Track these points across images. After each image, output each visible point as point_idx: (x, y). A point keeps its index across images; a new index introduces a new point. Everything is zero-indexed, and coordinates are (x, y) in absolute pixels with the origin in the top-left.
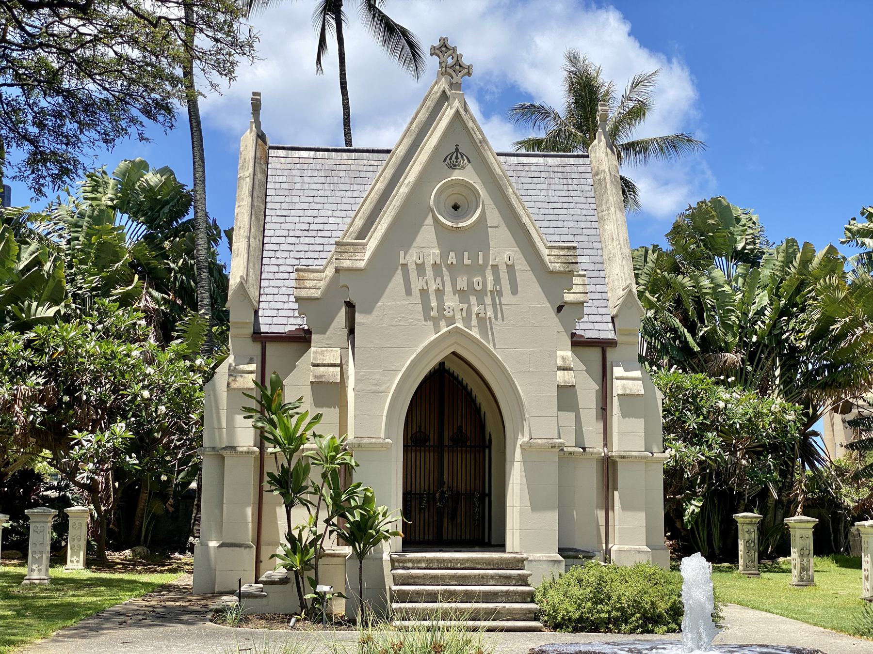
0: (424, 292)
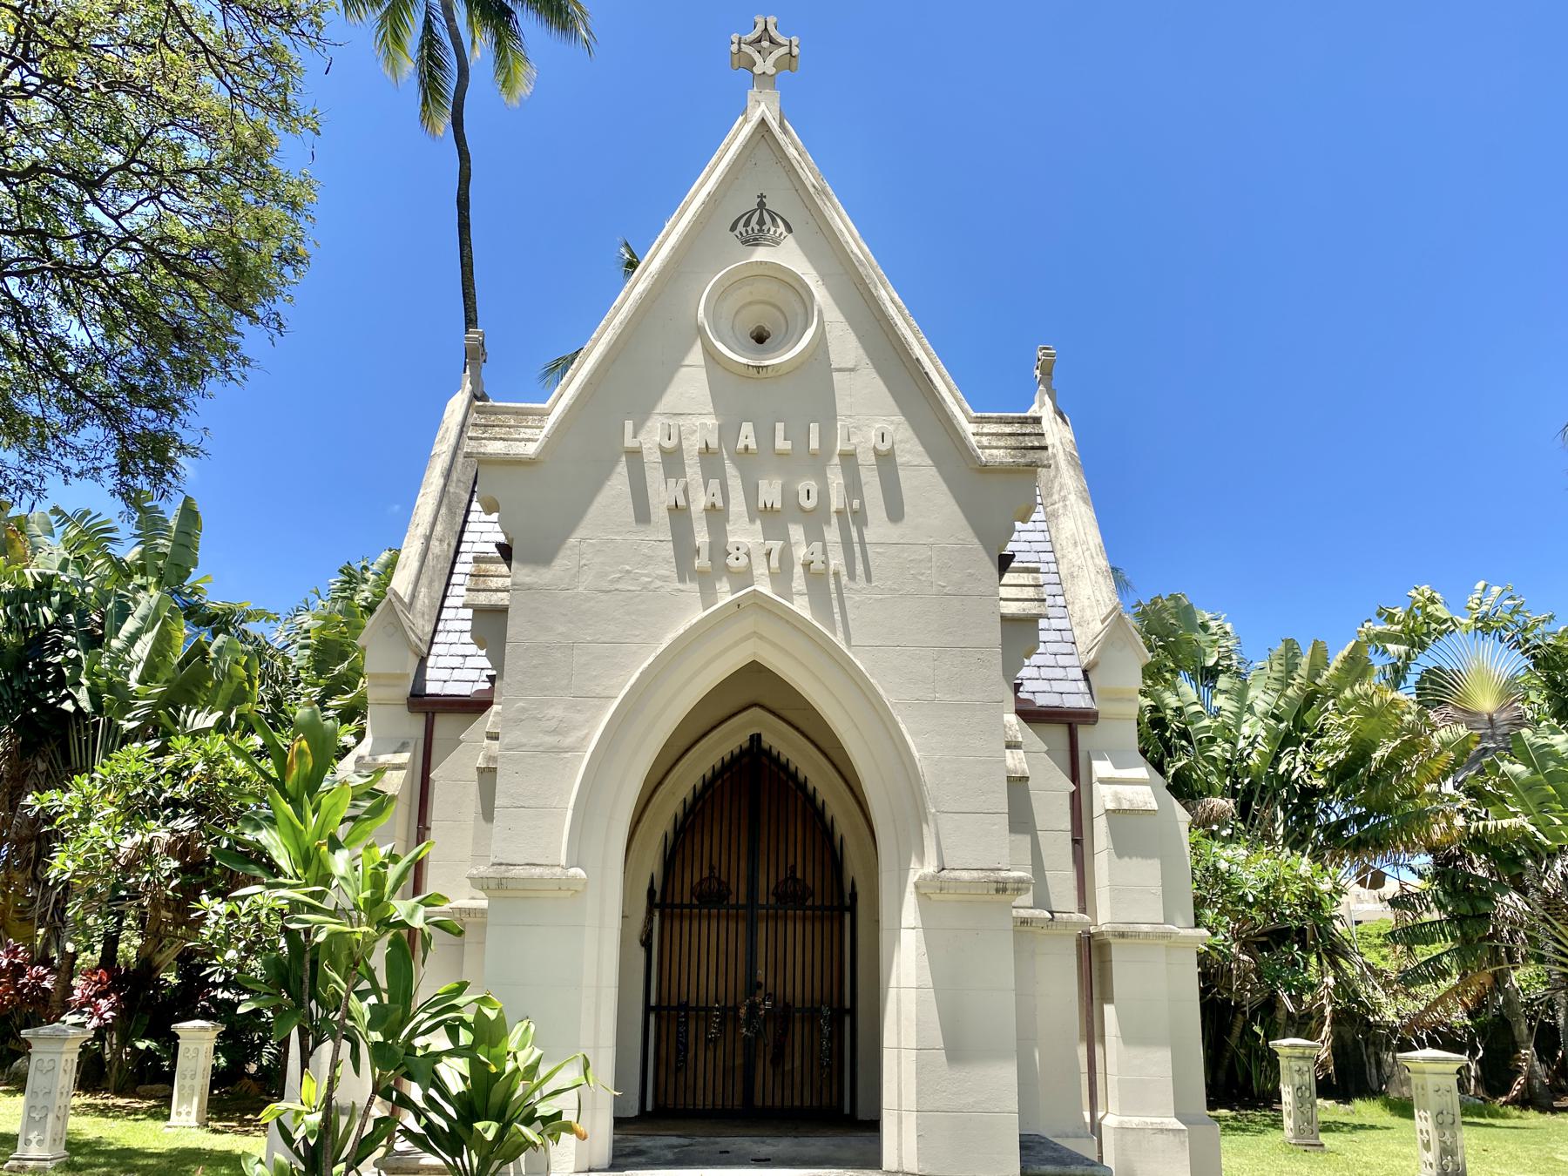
0: (679, 513)
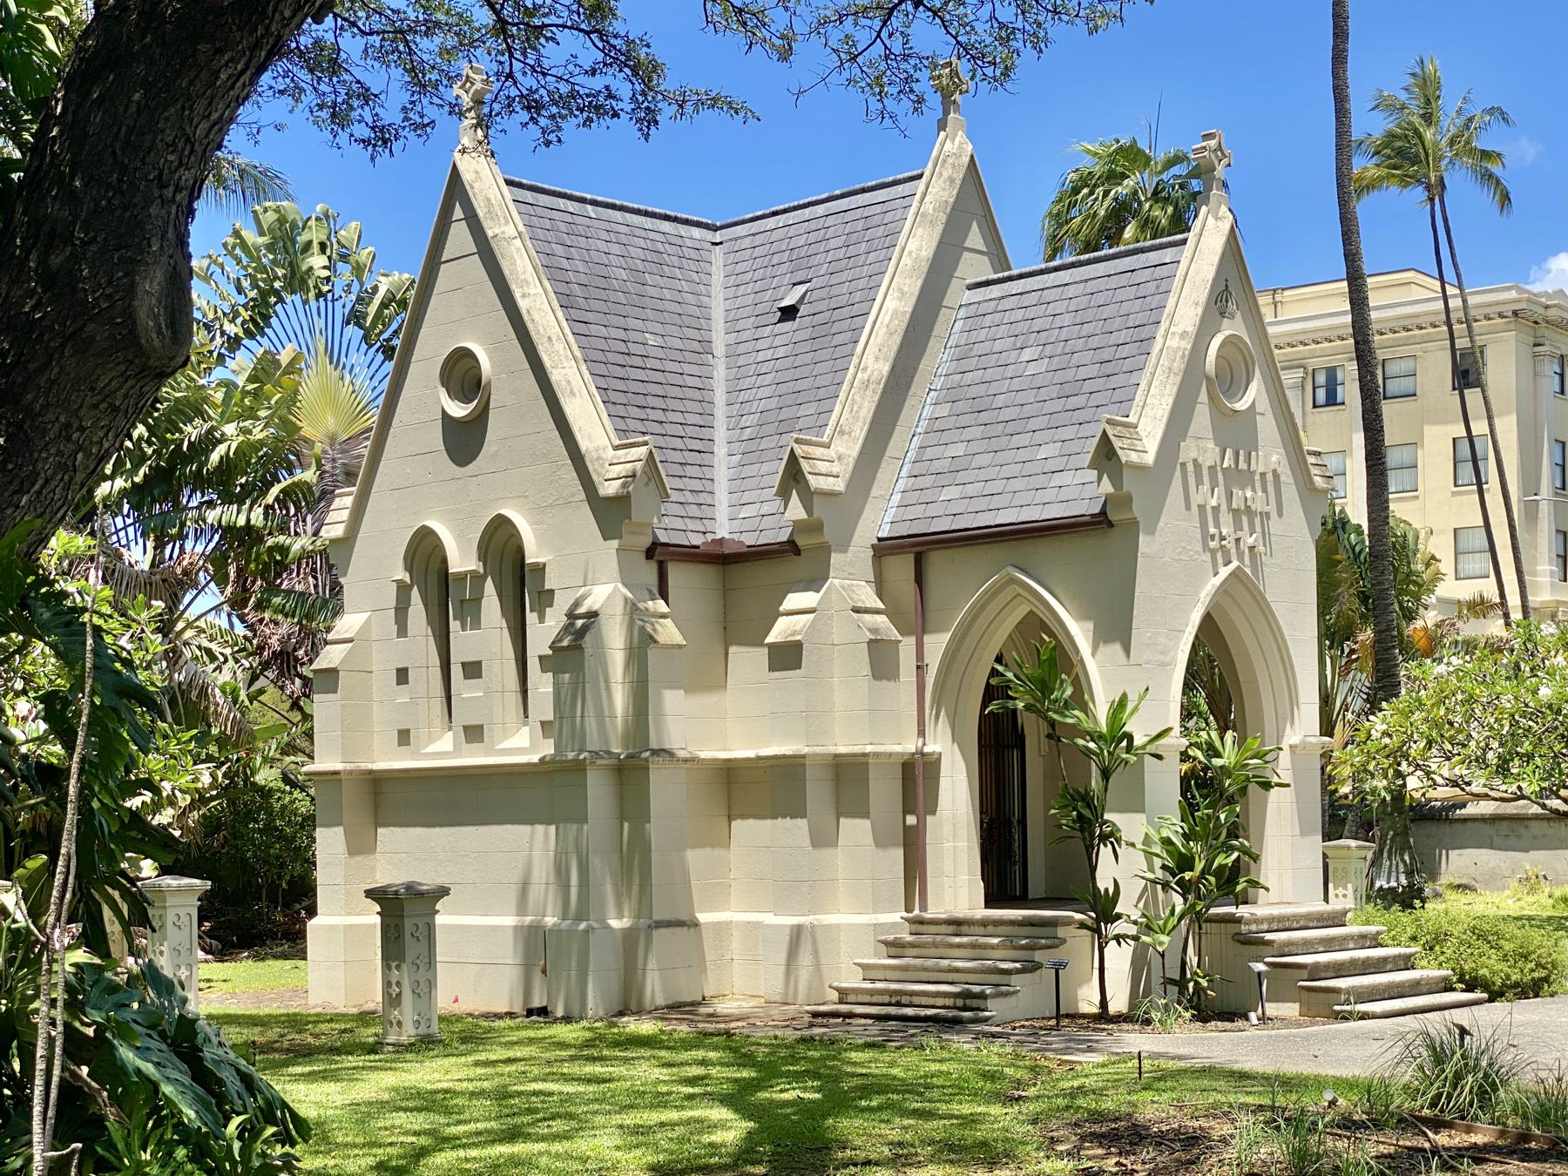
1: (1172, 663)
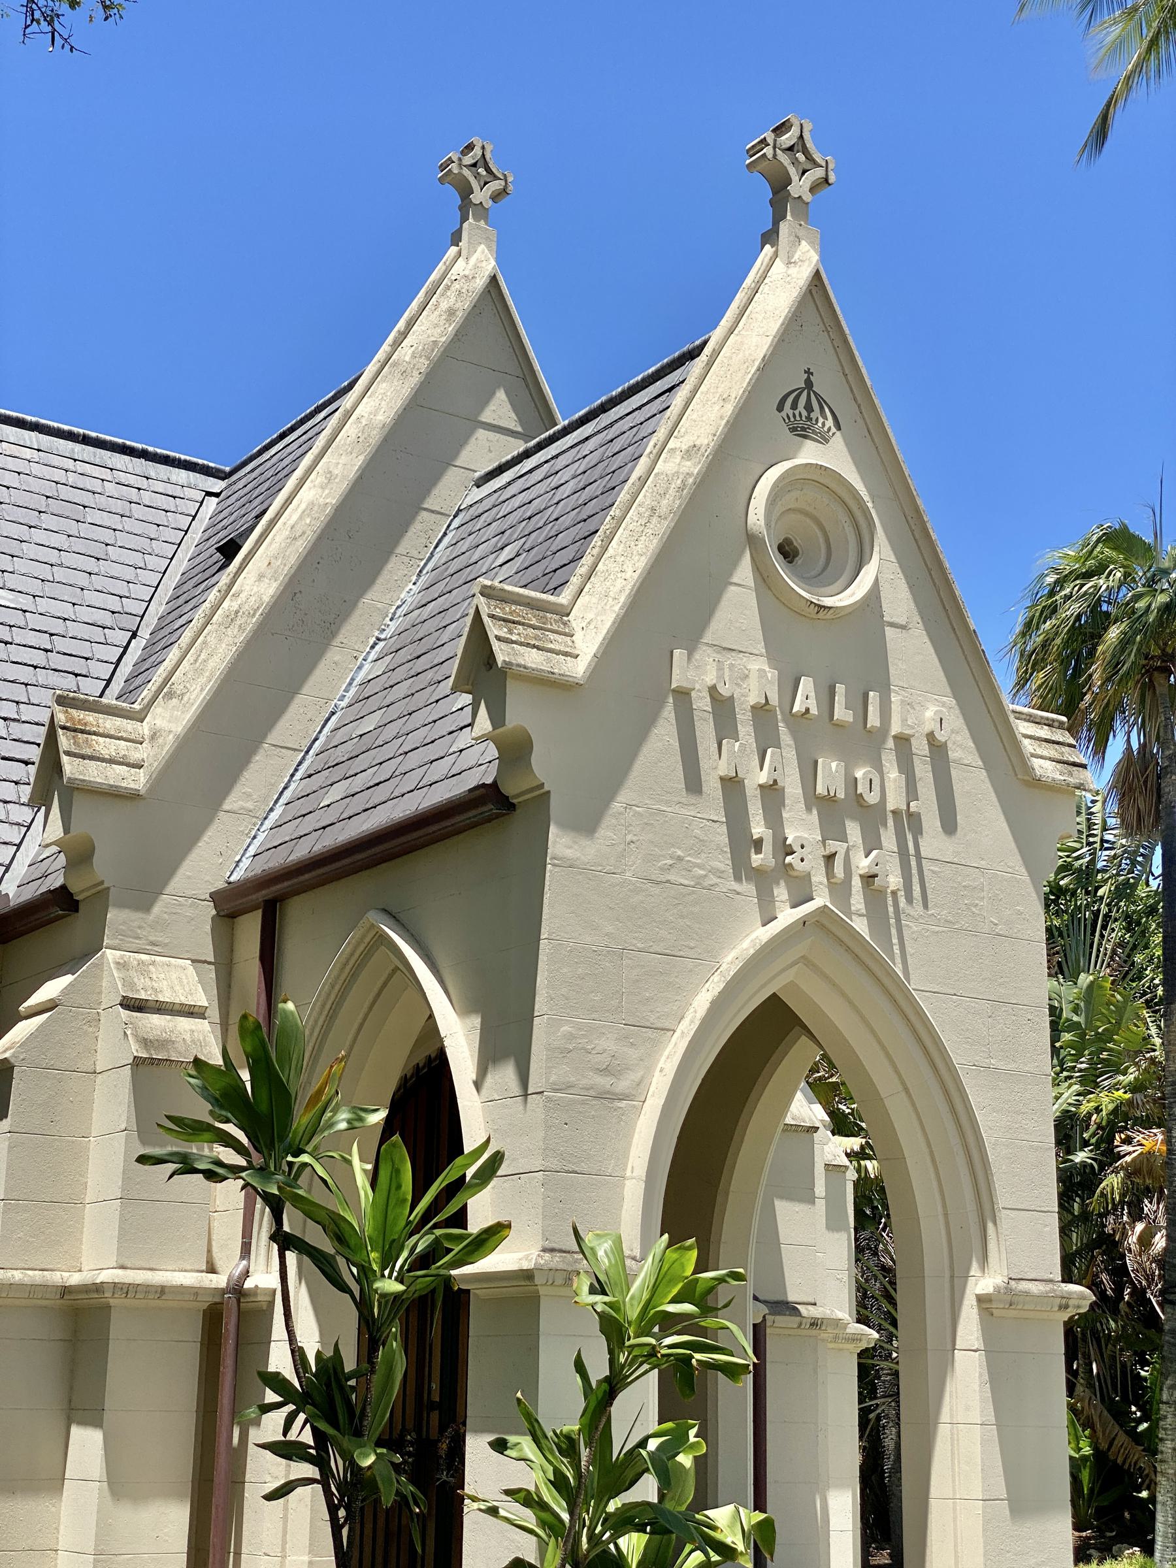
0: (732, 785)
1: (634, 1096)
